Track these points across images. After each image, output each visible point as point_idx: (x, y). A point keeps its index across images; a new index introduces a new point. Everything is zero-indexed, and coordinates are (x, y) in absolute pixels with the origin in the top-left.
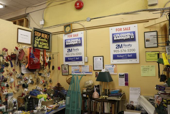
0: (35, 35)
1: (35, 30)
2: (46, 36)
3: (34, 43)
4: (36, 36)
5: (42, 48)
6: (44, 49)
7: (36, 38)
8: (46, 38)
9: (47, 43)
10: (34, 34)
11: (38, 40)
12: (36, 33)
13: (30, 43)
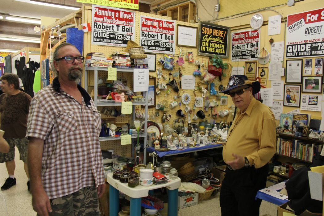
0: (203, 33)
1: (204, 25)
2: (221, 33)
3: (201, 45)
4: (204, 34)
5: (214, 52)
6: (217, 53)
7: (205, 38)
8: (220, 37)
9: (222, 44)
10: (202, 31)
11: (208, 40)
12: (204, 29)
13: (195, 45)
